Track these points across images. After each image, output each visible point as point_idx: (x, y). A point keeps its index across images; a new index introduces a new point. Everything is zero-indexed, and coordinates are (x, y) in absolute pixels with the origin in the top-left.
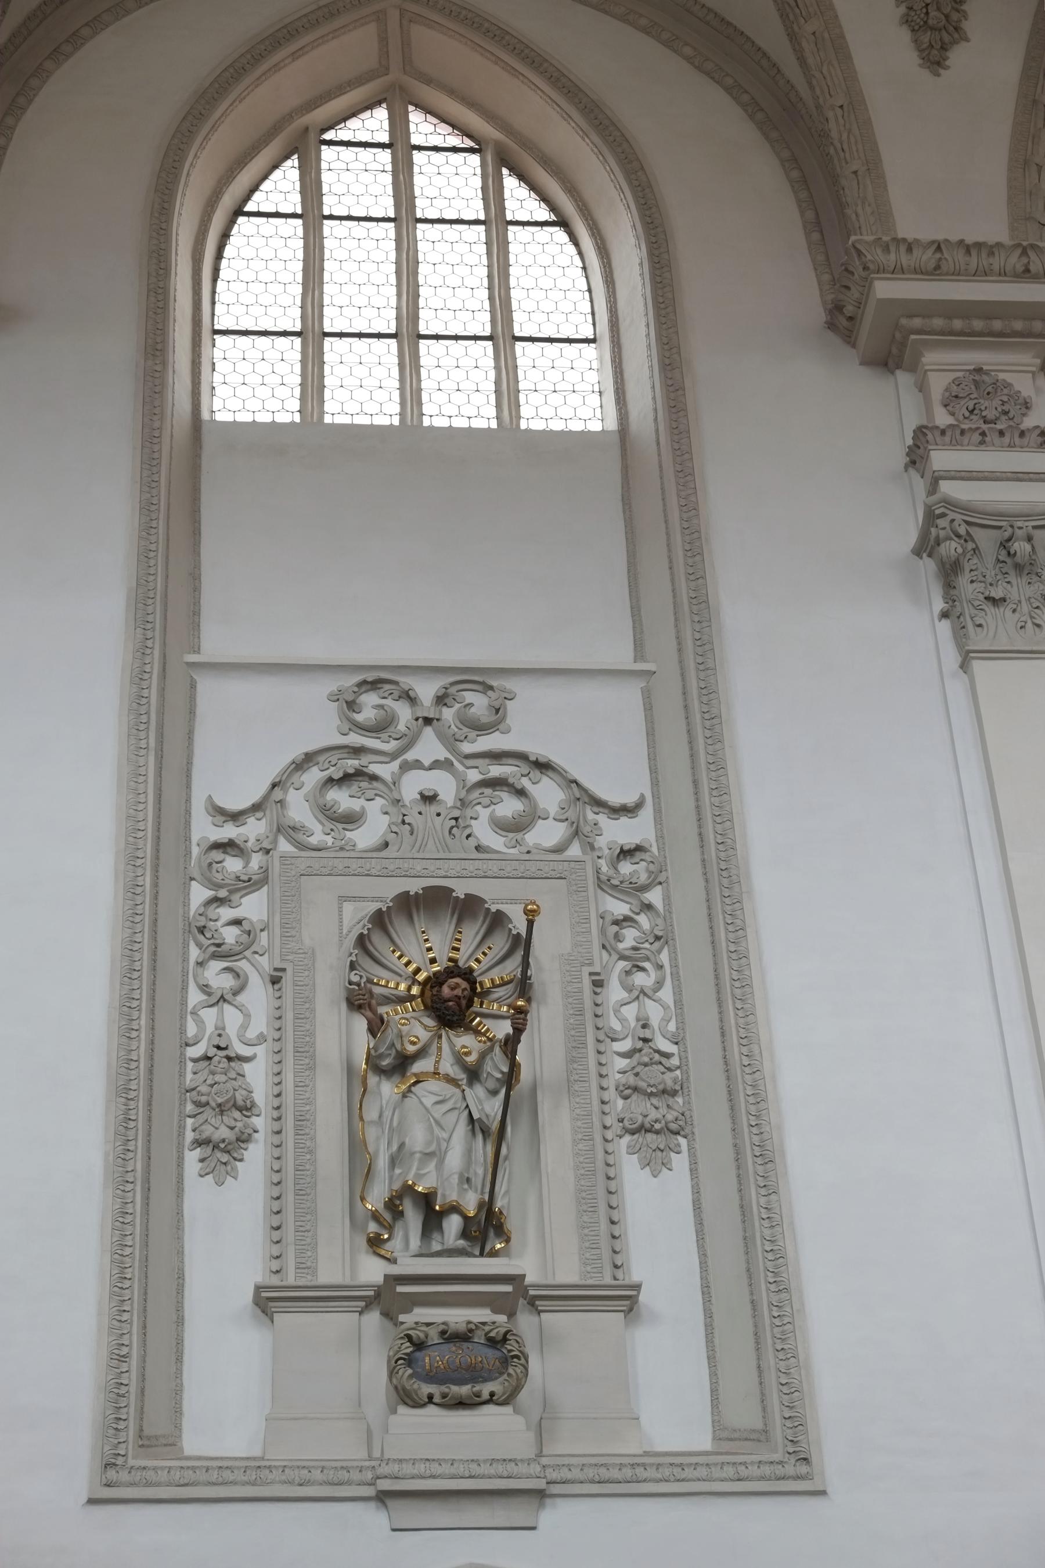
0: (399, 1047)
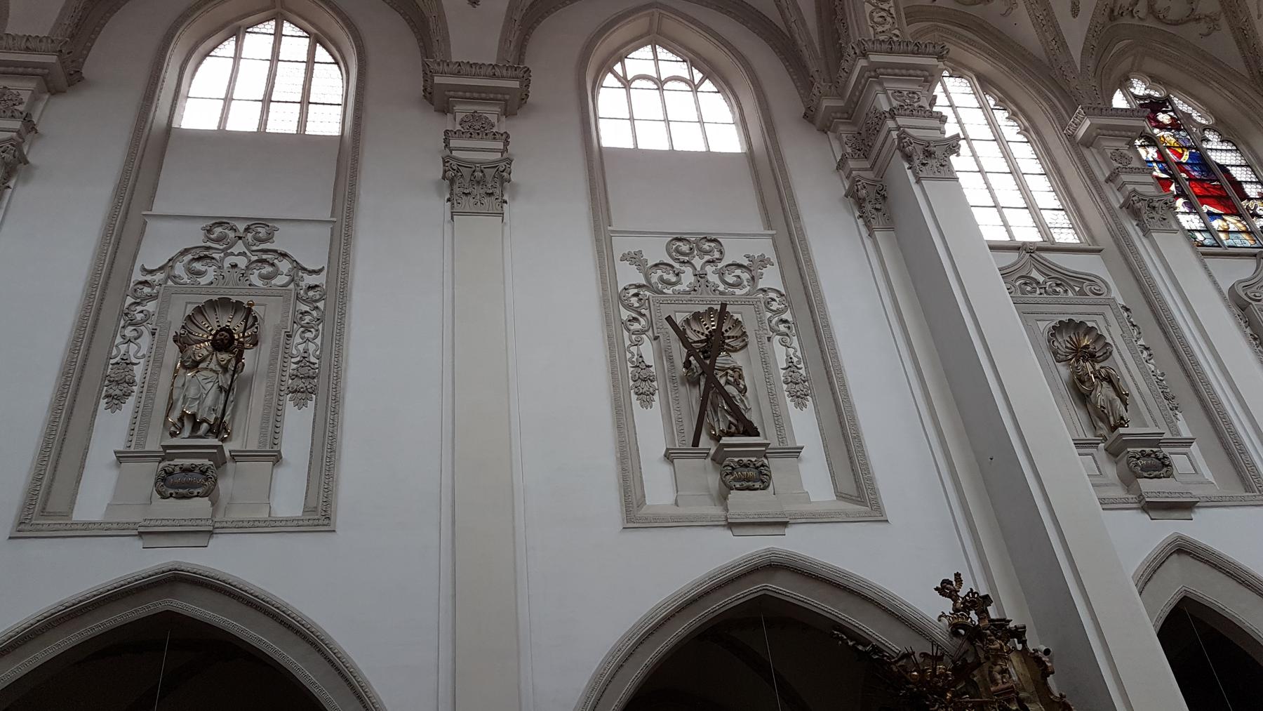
0: (193, 358)
